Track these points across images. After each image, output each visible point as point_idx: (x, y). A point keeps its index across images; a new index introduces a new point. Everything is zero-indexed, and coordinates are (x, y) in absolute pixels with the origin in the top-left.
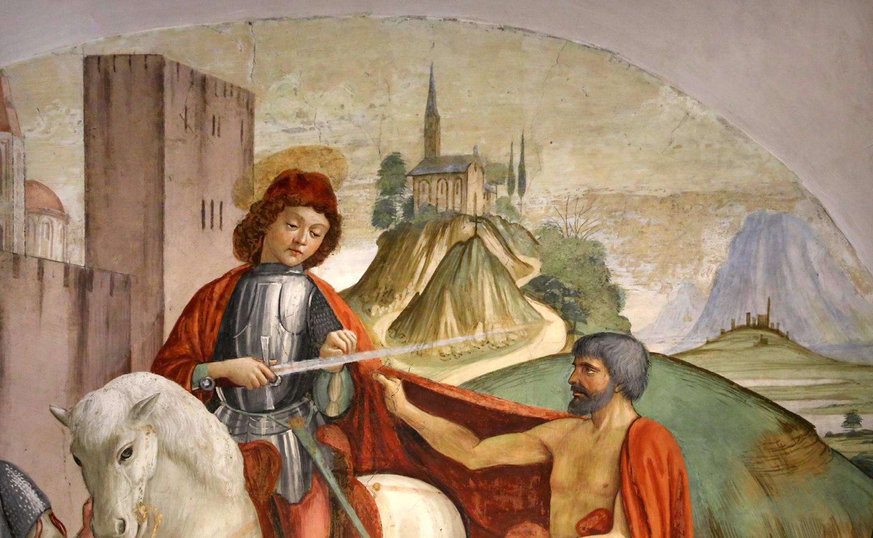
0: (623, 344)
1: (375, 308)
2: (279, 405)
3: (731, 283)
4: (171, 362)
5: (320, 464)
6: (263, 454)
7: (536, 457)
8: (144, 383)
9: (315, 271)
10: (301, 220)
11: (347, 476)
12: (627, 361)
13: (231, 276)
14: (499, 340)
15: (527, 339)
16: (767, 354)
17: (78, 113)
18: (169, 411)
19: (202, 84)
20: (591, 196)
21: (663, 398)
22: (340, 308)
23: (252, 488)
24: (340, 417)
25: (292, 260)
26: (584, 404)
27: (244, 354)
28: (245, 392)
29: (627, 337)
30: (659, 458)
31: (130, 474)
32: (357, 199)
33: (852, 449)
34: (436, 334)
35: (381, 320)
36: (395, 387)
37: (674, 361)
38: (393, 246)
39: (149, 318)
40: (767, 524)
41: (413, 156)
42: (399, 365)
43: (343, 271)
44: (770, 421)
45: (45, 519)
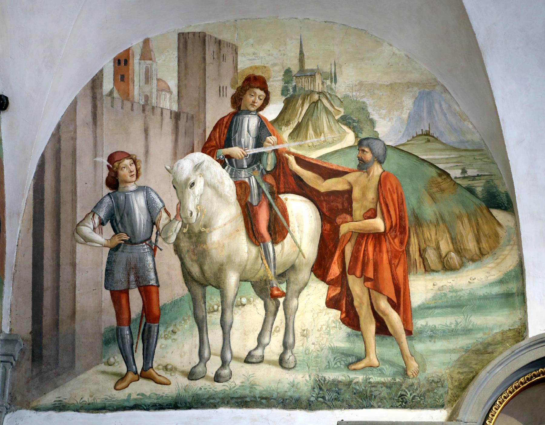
0: (377, 142)
1: (284, 128)
2: (249, 166)
3: (415, 117)
4: (209, 148)
5: (265, 190)
6: (243, 185)
7: (346, 187)
8: (199, 156)
9: (261, 113)
10: (255, 93)
11: (275, 194)
12: (379, 149)
13: (230, 115)
14: (330, 140)
15: (341, 139)
16: (430, 145)
17: (176, 54)
18: (208, 168)
19: (219, 43)
20: (361, 84)
21: (393, 163)
22: (270, 127)
23: (239, 199)
24: (271, 171)
25: (252, 109)
27: (235, 146)
28: (236, 160)
29: (378, 139)
30: (393, 187)
31: (194, 193)
32: (275, 85)
33: (465, 183)
34: (306, 138)
35: (286, 132)
36: (292, 159)
37: (396, 148)
38: (289, 103)
39: (201, 131)
40: (435, 214)
42: (293, 150)
43: (271, 113)
44: (433, 172)
45: (163, 210)
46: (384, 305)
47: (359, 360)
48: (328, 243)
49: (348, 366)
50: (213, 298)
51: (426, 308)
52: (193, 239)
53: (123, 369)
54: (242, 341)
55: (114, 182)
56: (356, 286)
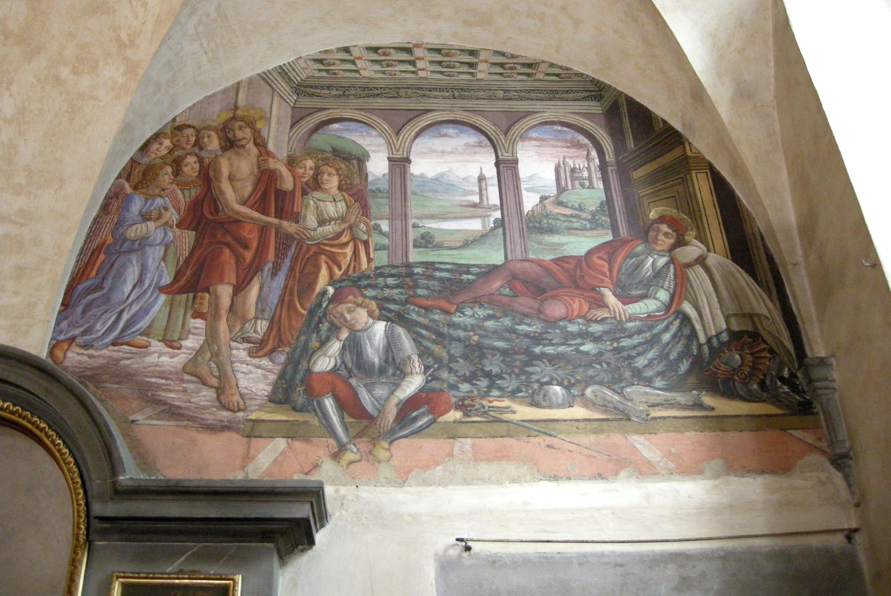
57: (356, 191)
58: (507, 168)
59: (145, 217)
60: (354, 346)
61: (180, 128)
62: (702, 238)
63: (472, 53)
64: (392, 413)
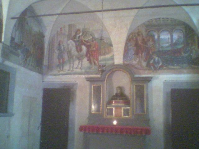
4: (72, 39)
8: (71, 41)
26: (93, 41)
38: (83, 32)
41: (84, 27)
43: (81, 34)
46: (95, 60)
47: (91, 68)
48: (88, 51)
49: (90, 69)
50: (72, 60)
51: (101, 61)
52: (69, 52)
53: (59, 70)
54: (75, 66)
55: (59, 45)
56: (92, 58)
57: (154, 41)
58: (172, 36)
59: (131, 46)
60: (154, 60)
61: (133, 33)
62: (195, 46)
63: (168, 18)
64: (158, 67)
